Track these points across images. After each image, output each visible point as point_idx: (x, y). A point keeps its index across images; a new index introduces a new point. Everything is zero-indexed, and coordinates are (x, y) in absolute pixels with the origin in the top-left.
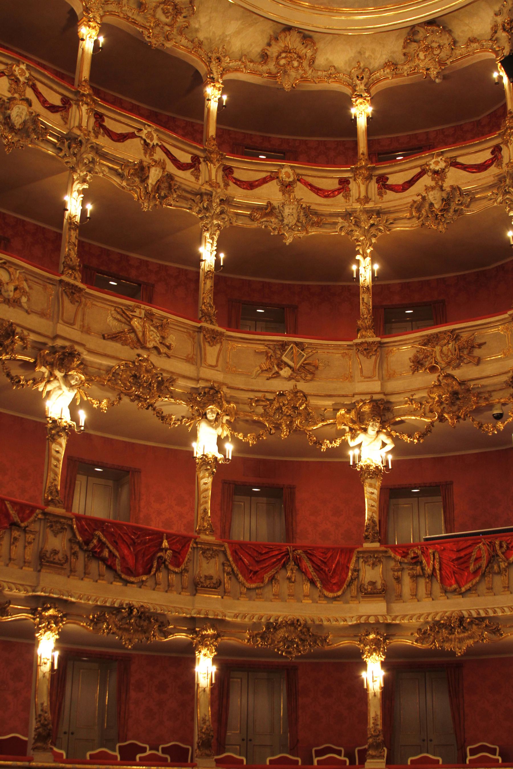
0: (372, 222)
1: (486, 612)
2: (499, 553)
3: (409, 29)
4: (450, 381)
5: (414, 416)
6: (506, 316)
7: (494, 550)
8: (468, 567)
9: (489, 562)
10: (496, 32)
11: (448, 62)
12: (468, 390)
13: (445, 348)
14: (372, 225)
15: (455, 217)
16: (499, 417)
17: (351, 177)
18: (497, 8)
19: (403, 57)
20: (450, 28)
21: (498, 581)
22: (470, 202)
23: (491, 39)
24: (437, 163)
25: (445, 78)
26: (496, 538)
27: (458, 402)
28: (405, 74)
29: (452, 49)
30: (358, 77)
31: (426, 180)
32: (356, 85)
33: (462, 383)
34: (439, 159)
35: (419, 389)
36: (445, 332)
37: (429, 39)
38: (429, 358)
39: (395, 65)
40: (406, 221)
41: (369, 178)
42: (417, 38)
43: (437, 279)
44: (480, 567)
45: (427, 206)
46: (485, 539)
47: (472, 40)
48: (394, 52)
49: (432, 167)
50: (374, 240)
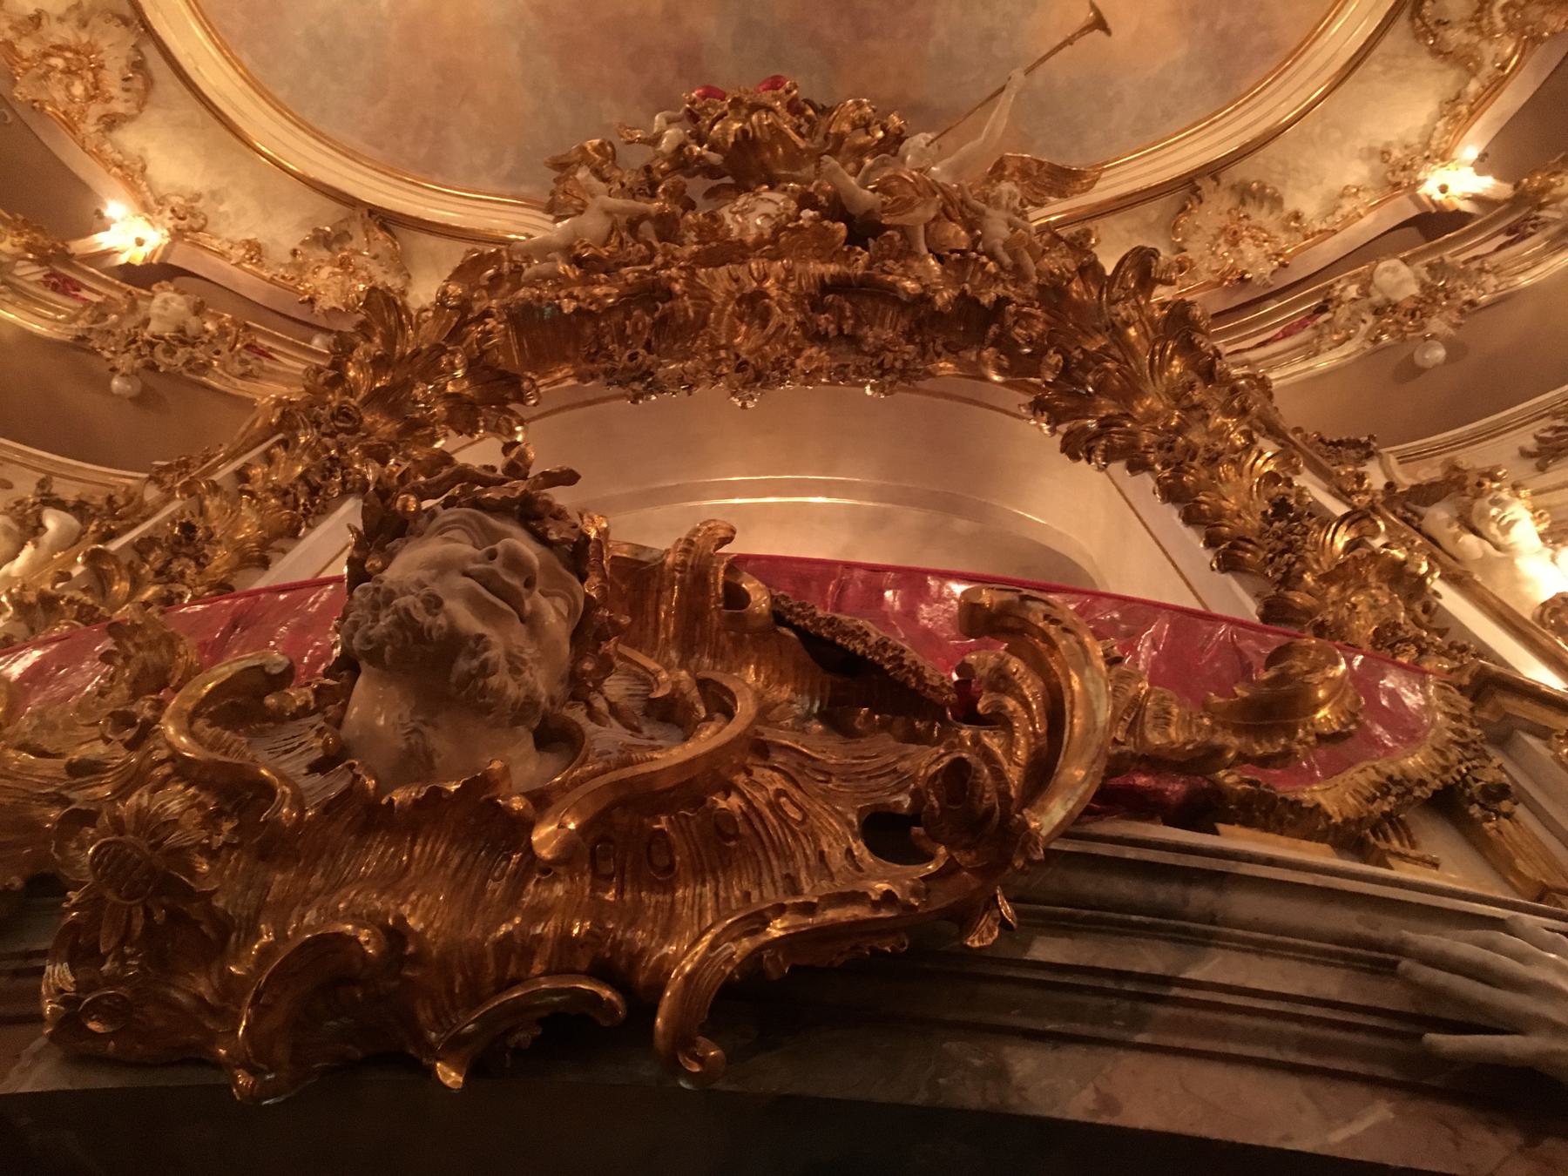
19: (289, 259)
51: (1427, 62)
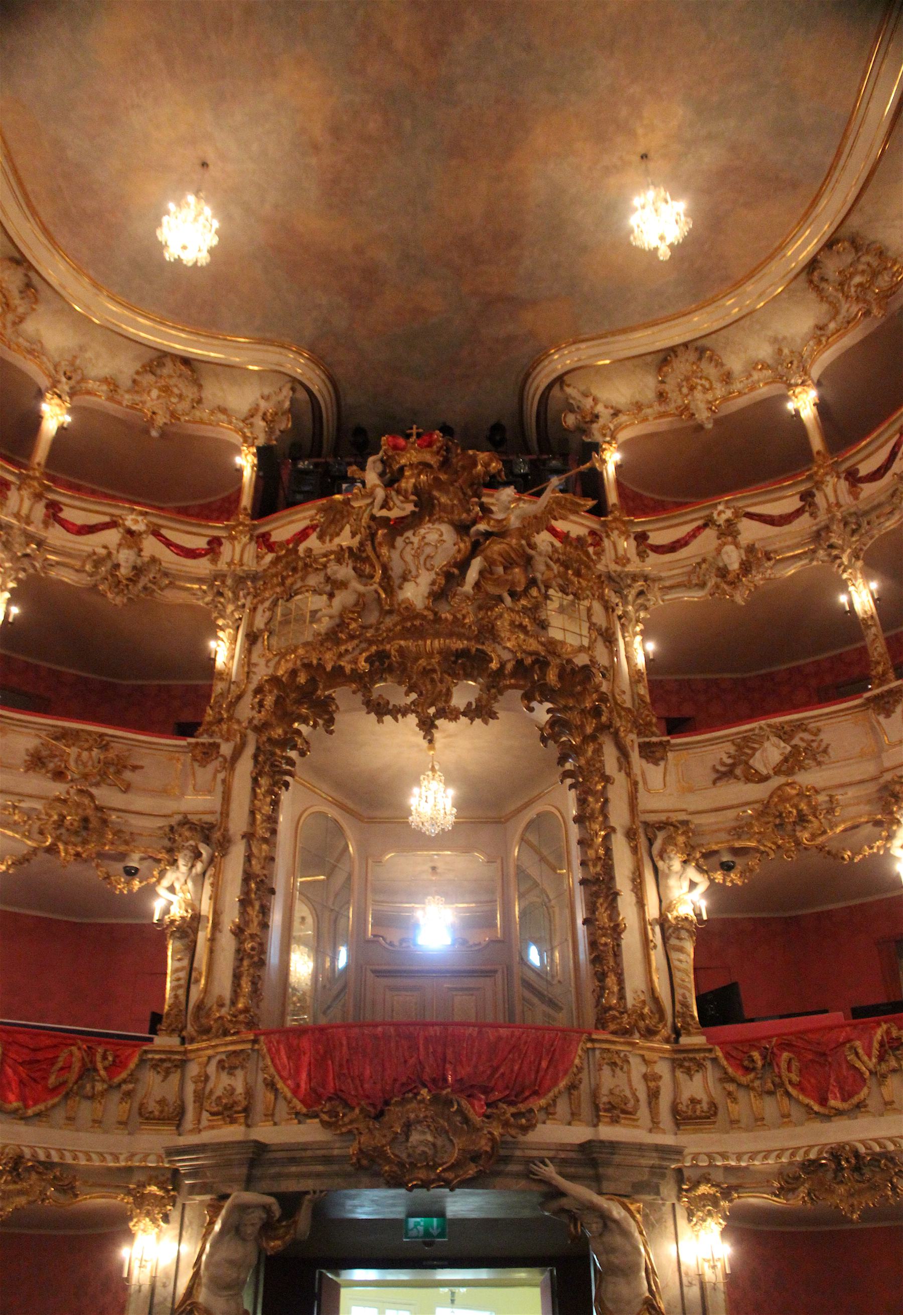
0: (28, 551)
1: (62, 1157)
2: (100, 1066)
3: (158, 354)
4: (86, 801)
5: (13, 831)
6: (183, 743)
7: (93, 1062)
8: (45, 1078)
9: (80, 1077)
10: (252, 416)
11: (182, 418)
12: (105, 822)
13: (85, 754)
14: (27, 555)
15: (142, 595)
16: (131, 873)
17: (14, 483)
18: (266, 391)
19: (129, 383)
20: (202, 383)
21: (85, 1110)
22: (167, 586)
23: (243, 421)
24: (135, 521)
25: (164, 435)
26: (100, 1044)
27: (84, 833)
28: (125, 403)
29: (193, 407)
30: (65, 374)
31: (112, 537)
32: (59, 382)
33: (99, 809)
34: (140, 518)
35: (30, 796)
36: (89, 733)
37: (172, 382)
38: (56, 760)
39: (116, 387)
40: (71, 571)
41: (38, 496)
42: (158, 372)
43: (49, 669)
44: (64, 1083)
45: (109, 565)
46: (82, 1040)
47: (223, 410)
48: (121, 372)
49: (129, 523)
50: (22, 575)
51: (812, 296)
